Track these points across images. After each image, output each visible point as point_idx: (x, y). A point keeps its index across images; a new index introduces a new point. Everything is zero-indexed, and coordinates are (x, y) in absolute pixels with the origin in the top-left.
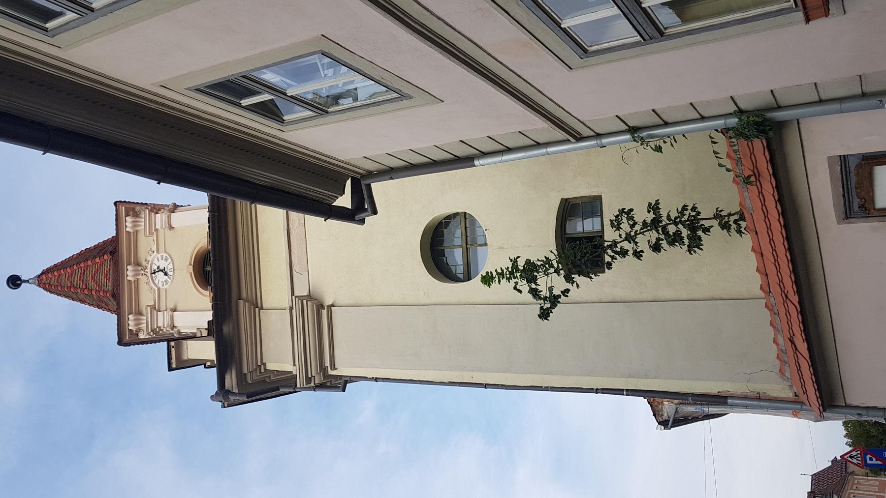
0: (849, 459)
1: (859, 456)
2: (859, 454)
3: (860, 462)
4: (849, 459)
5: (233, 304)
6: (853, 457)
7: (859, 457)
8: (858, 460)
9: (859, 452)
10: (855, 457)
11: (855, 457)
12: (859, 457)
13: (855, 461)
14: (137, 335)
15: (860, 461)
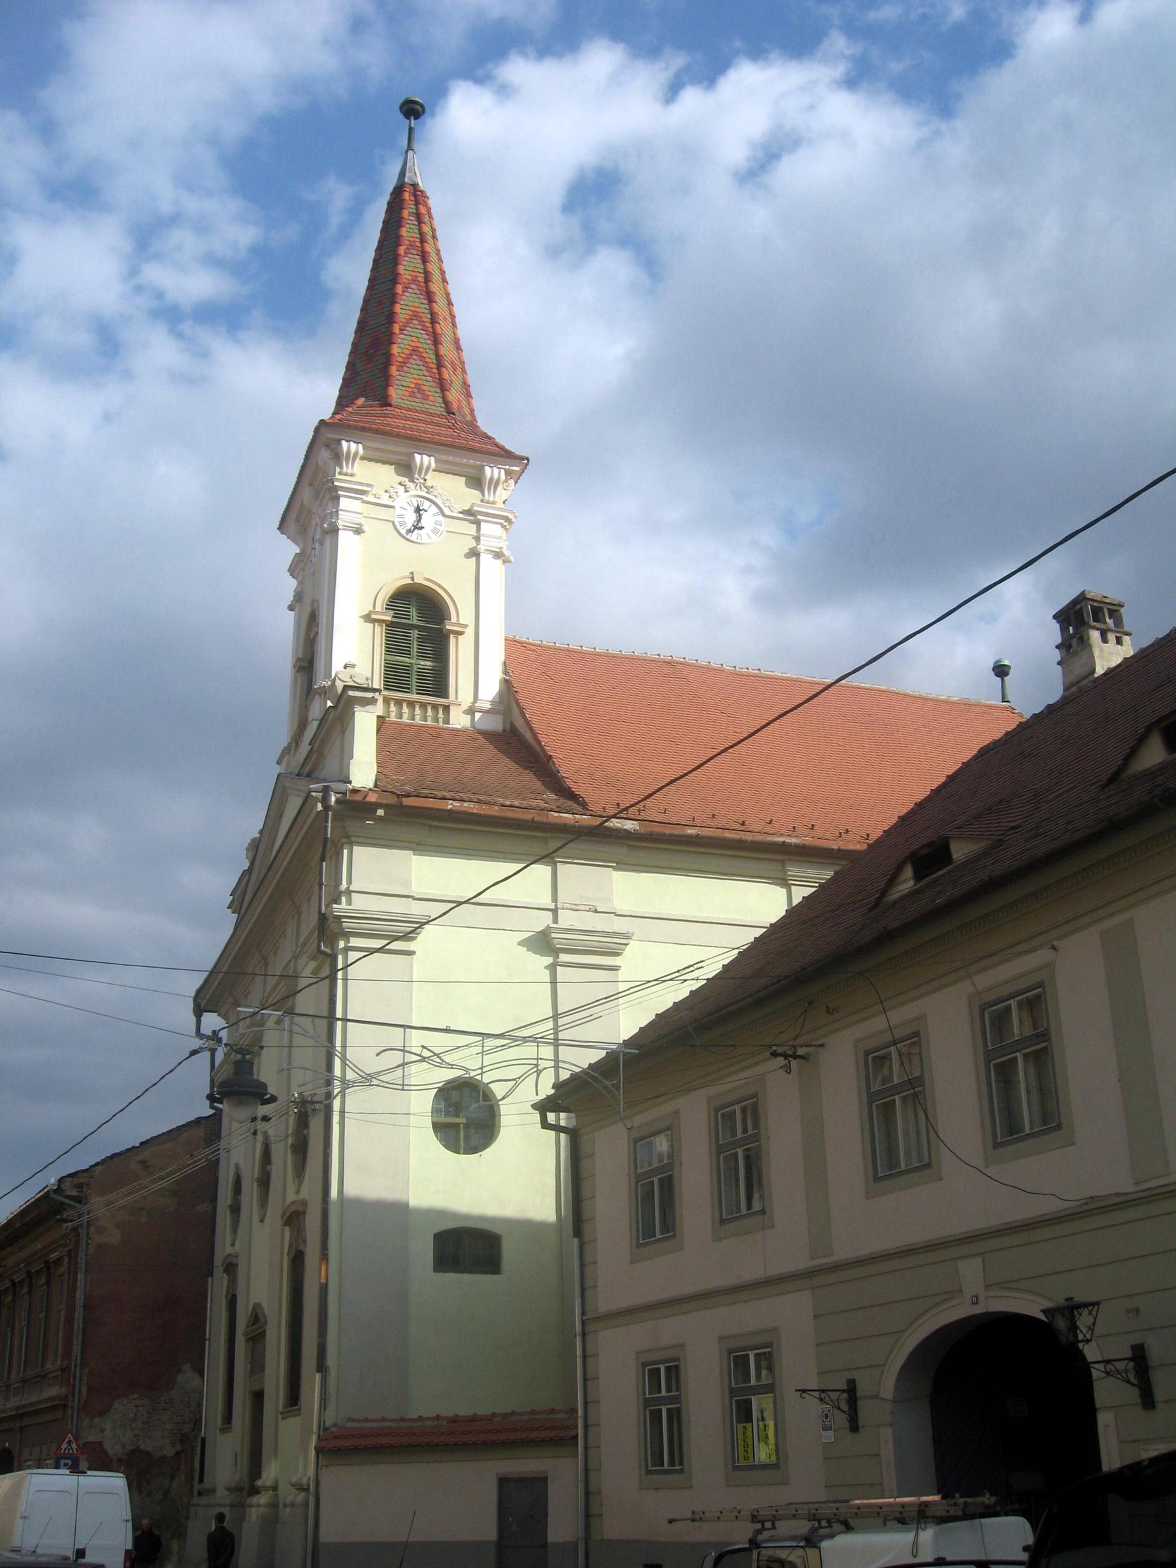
0: (67, 1440)
1: (71, 1451)
2: (73, 1451)
3: (62, 1452)
4: (67, 1440)
5: (425, 821)
6: (70, 1444)
7: (69, 1451)
8: (66, 1449)
9: (75, 1451)
10: (69, 1447)
11: (69, 1447)
12: (69, 1451)
13: (64, 1445)
14: (327, 446)
15: (64, 1451)
